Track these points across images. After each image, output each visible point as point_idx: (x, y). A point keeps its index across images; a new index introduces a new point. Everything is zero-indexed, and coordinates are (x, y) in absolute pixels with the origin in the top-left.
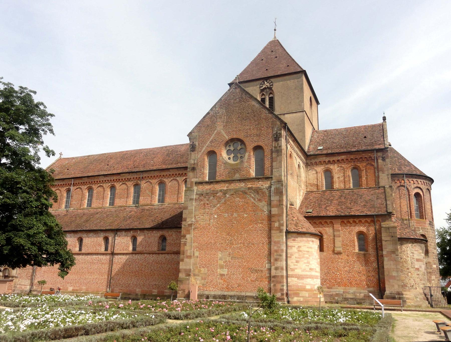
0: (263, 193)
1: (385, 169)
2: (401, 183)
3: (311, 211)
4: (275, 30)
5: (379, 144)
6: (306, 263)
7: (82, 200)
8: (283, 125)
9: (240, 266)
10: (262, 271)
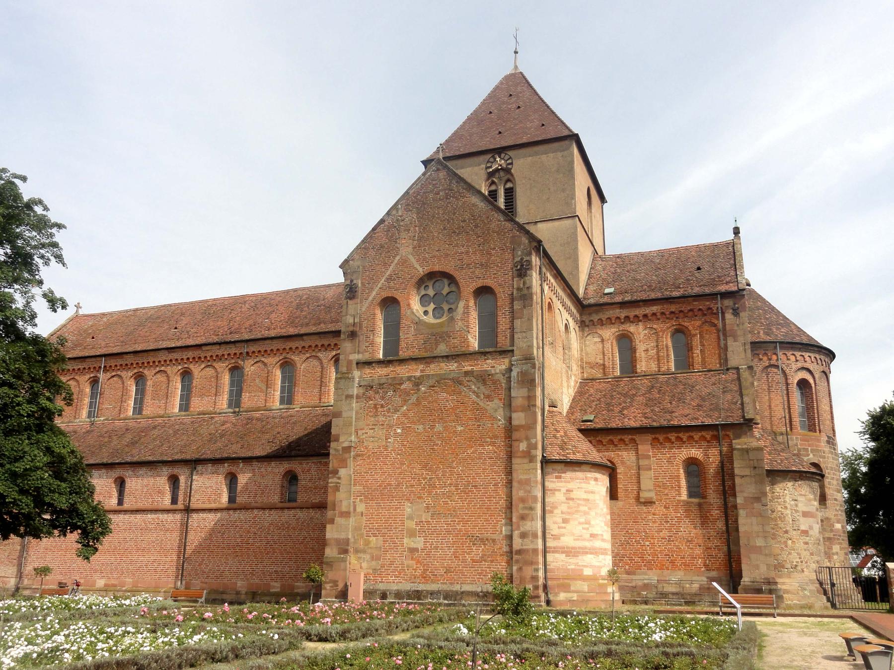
0: (495, 382)
1: (739, 333)
2: (770, 359)
3: (591, 417)
4: (516, 52)
5: (727, 283)
7: (123, 400)
8: (535, 244)
9: (449, 532)
10: (494, 540)
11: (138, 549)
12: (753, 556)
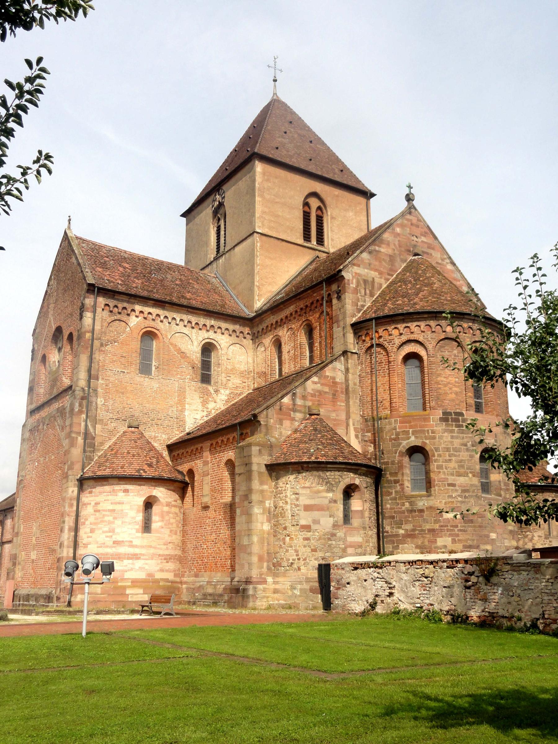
1: (341, 317)
2: (372, 339)
6: (106, 532)
12: (242, 555)
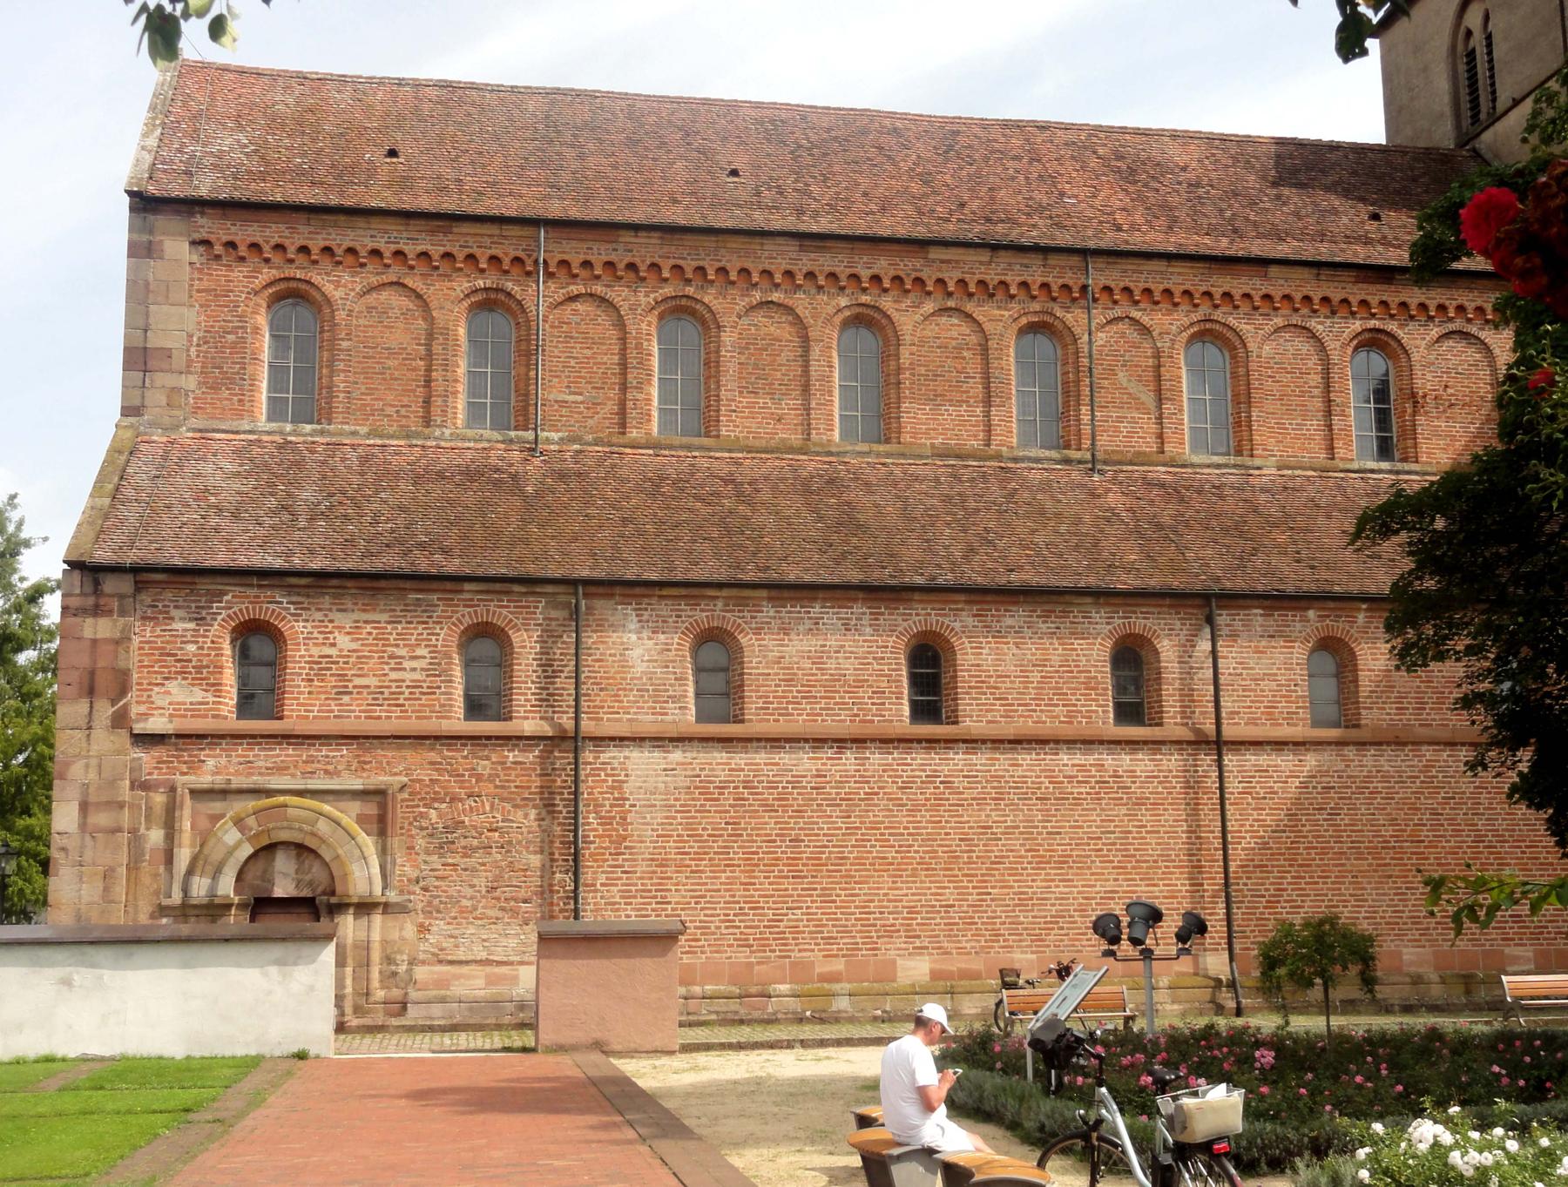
11: (1041, 863)
